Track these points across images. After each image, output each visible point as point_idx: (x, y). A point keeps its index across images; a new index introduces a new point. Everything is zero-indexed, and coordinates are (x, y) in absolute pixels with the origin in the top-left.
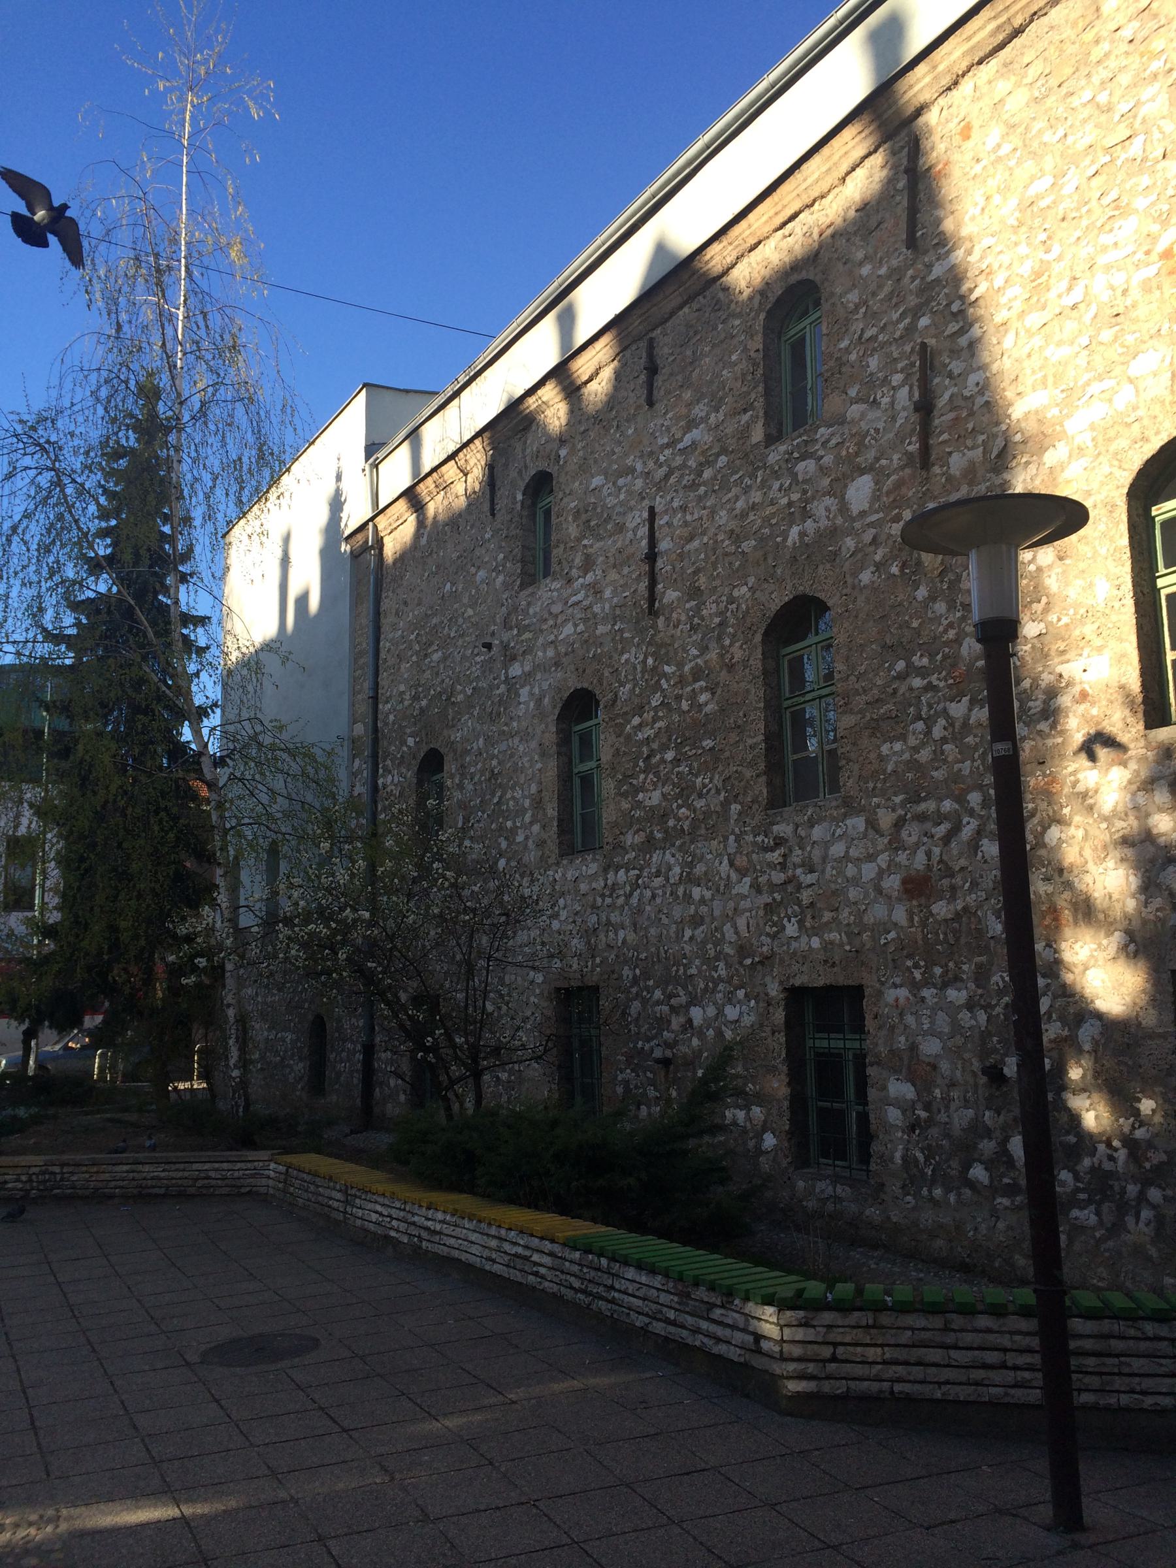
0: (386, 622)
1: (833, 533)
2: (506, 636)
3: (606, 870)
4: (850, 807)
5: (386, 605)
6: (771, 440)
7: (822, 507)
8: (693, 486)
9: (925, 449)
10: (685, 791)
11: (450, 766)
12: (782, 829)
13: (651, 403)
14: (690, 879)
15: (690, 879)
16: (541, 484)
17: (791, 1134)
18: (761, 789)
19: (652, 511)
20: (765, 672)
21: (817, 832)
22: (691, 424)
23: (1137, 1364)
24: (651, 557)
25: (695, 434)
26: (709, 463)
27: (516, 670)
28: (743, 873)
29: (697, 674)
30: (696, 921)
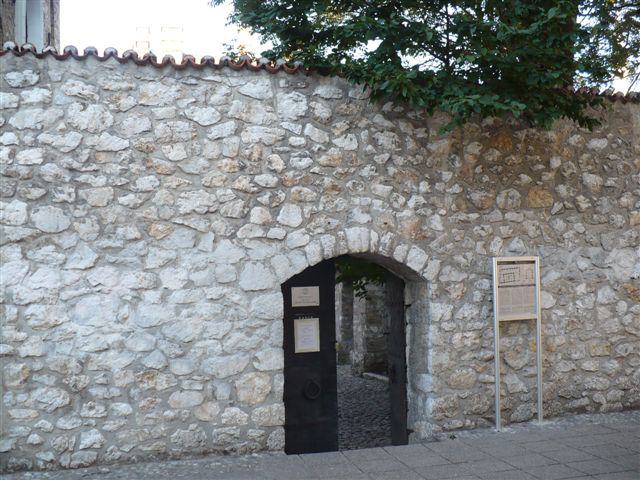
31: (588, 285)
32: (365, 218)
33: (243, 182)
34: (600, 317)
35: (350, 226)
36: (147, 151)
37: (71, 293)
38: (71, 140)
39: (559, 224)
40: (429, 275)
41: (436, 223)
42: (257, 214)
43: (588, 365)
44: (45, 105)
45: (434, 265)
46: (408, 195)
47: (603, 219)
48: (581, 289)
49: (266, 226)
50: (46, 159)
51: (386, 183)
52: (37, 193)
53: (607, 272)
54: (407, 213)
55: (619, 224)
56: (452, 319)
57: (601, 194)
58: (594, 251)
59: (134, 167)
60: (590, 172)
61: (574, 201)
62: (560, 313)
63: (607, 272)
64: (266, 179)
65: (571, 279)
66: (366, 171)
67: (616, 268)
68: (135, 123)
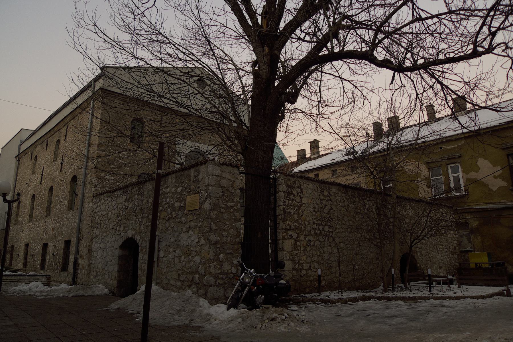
0: (18, 175)
1: (55, 177)
2: (29, 182)
3: (32, 224)
4: (51, 218)
5: (19, 172)
6: (54, 161)
7: (55, 173)
8: (47, 165)
9: (61, 169)
10: (40, 212)
11: (21, 204)
12: (46, 220)
13: (46, 150)
14: (38, 227)
15: (38, 227)
16: (36, 157)
17: (41, 265)
18: (45, 214)
19: (44, 167)
20: (48, 196)
21: (48, 221)
22: (49, 155)
23: (26, 281)
24: (42, 175)
25: (49, 157)
26: (49, 162)
27: (29, 189)
28: (43, 226)
29: (43, 195)
30: (38, 233)
31: (174, 248)
32: (131, 227)
33: (117, 220)
34: (176, 262)
35: (129, 229)
36: (108, 214)
37: (98, 249)
38: (100, 214)
39: (167, 224)
40: (139, 244)
41: (142, 228)
42: (118, 227)
43: (172, 282)
44: (99, 206)
45: (141, 240)
46: (139, 219)
47: (179, 220)
48: (171, 250)
49: (119, 231)
50: (98, 218)
51: (135, 216)
52: (97, 226)
53: (179, 243)
54: (138, 224)
55: (184, 222)
56: (142, 259)
57: (179, 210)
58: (177, 234)
59: (106, 218)
60: (177, 202)
61: (171, 214)
62: (165, 259)
63: (179, 243)
64: (120, 218)
65: (169, 246)
66: (133, 214)
67: (182, 241)
68: (107, 208)
